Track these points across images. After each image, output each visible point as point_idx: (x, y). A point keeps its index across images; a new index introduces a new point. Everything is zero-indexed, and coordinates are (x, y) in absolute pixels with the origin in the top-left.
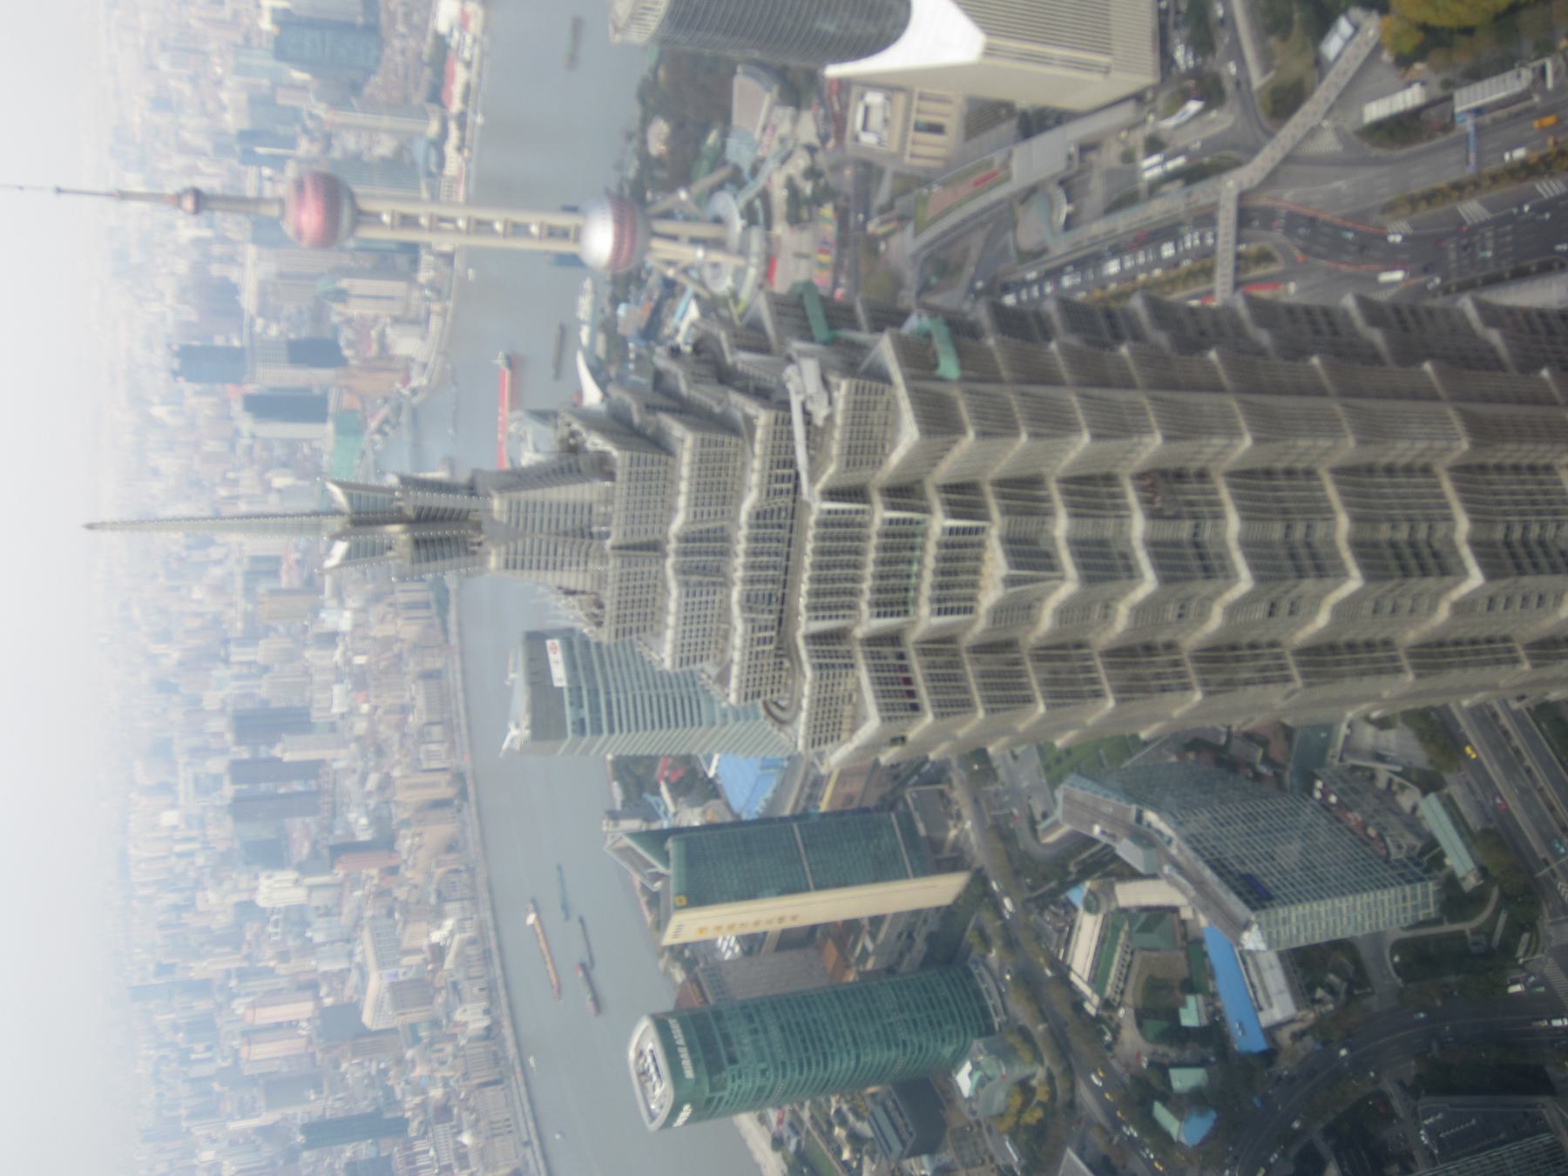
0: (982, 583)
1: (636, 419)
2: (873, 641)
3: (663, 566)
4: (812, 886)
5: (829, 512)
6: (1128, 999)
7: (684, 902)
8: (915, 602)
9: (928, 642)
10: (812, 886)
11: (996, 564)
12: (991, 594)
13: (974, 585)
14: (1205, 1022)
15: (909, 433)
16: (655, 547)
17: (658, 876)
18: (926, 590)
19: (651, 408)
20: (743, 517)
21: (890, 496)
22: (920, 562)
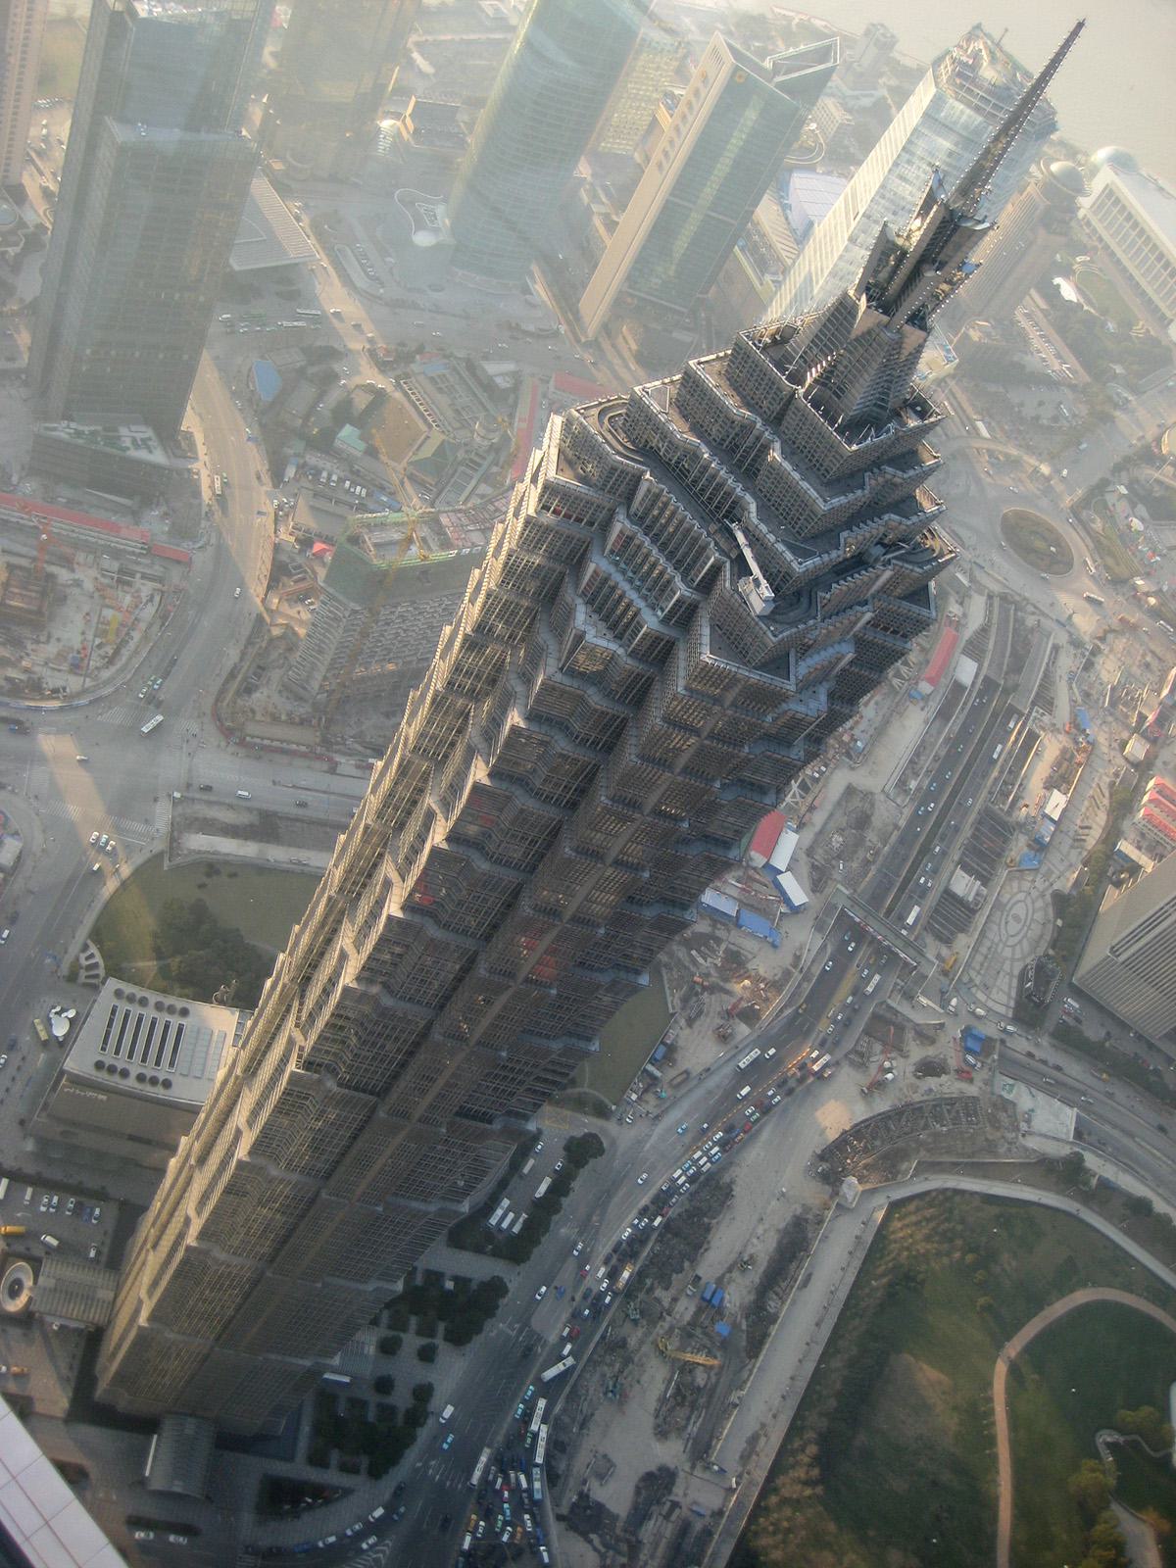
0: (595, 617)
1: (890, 470)
2: (612, 513)
3: (761, 416)
4: (672, 199)
5: (709, 559)
6: (398, 395)
7: (736, 79)
8: (616, 564)
9: (586, 550)
10: (672, 199)
11: (599, 639)
12: (581, 616)
13: (598, 611)
14: (337, 443)
15: (707, 657)
16: (776, 421)
17: (777, 69)
18: (617, 577)
19: (891, 485)
20: (748, 497)
21: (690, 605)
22: (638, 589)
